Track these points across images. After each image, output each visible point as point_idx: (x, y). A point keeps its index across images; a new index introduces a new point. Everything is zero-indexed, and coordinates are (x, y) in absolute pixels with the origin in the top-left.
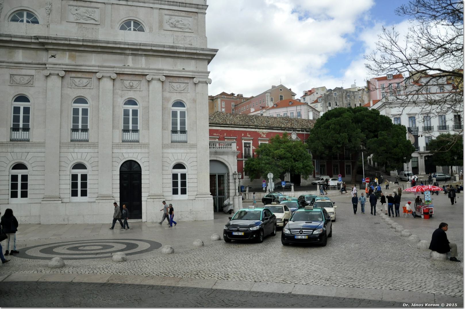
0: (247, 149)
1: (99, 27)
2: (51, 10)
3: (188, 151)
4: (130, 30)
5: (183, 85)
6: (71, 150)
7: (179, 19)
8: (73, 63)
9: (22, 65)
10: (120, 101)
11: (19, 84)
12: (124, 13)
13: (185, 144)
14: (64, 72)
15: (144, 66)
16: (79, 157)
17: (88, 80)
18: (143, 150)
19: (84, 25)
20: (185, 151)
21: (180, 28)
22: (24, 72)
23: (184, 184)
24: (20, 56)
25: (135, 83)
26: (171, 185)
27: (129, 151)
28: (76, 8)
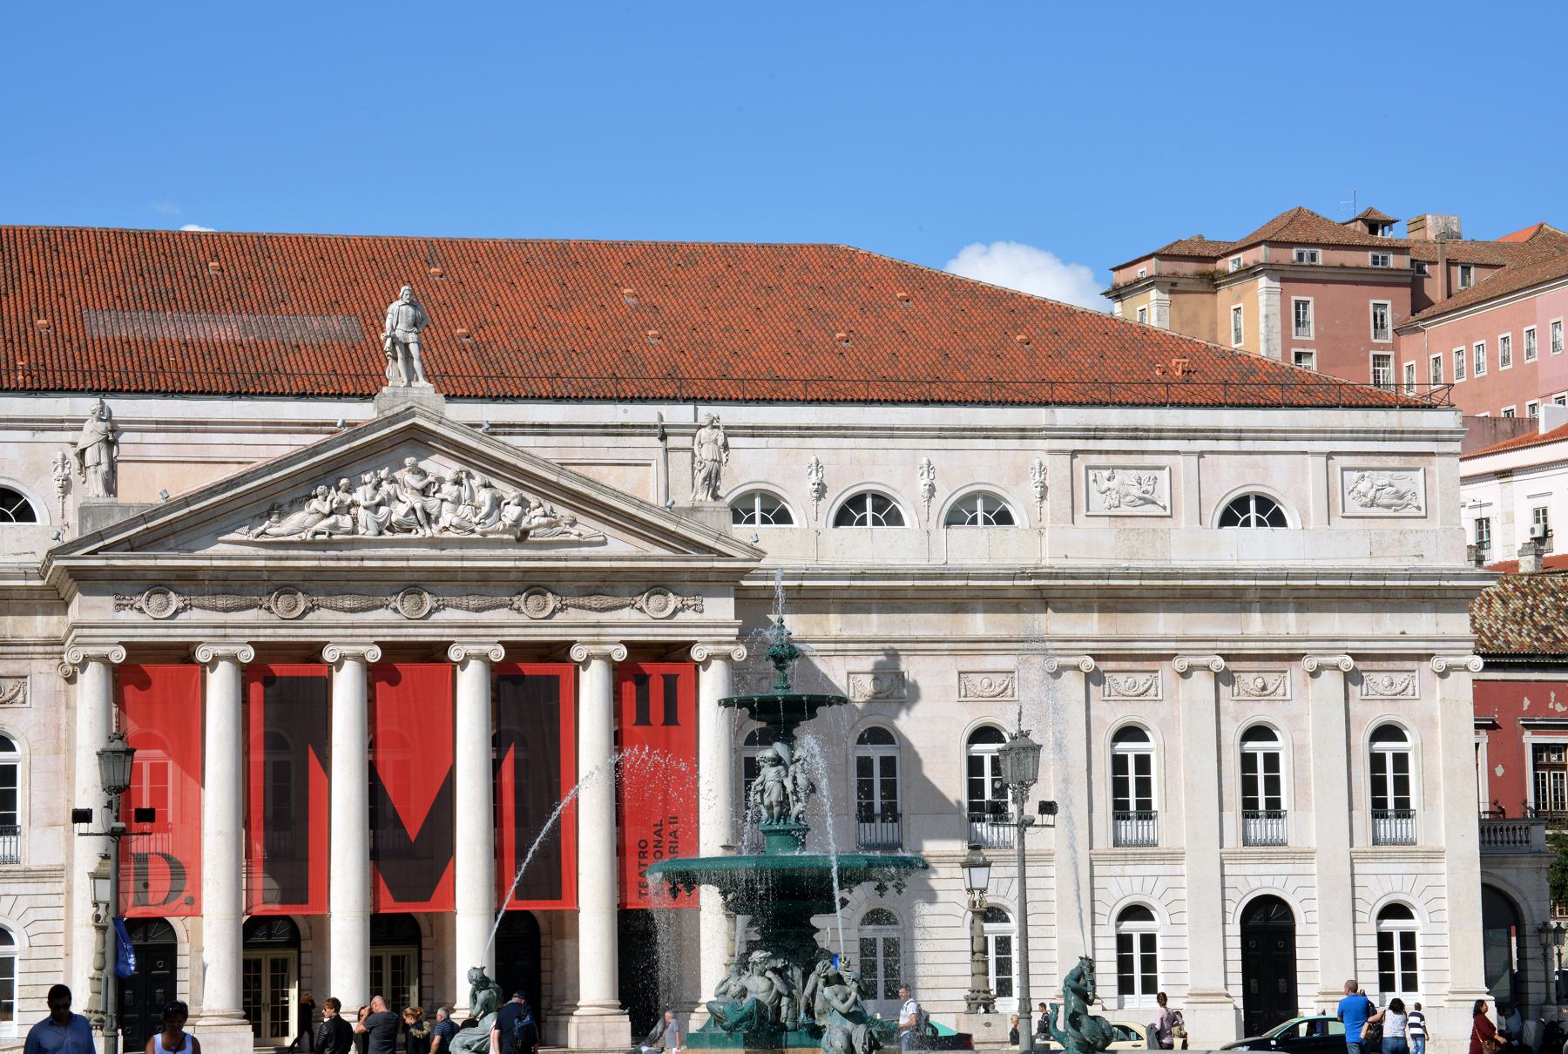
0: (1549, 776)
1: (1169, 522)
2: (1045, 488)
3: (1421, 868)
4: (1247, 523)
5: (1399, 678)
6: (1117, 870)
7: (1383, 478)
8: (1111, 632)
9: (986, 646)
10: (1233, 733)
11: (981, 699)
12: (1231, 476)
13: (1412, 848)
14: (1091, 660)
15: (1293, 631)
16: (1137, 889)
17: (1147, 676)
18: (1300, 868)
19: (1129, 523)
20: (1412, 868)
21: (1388, 507)
22: (990, 662)
23: (1409, 961)
24: (978, 624)
25: (1271, 680)
26: (1376, 964)
27: (1263, 869)
28: (1106, 473)
